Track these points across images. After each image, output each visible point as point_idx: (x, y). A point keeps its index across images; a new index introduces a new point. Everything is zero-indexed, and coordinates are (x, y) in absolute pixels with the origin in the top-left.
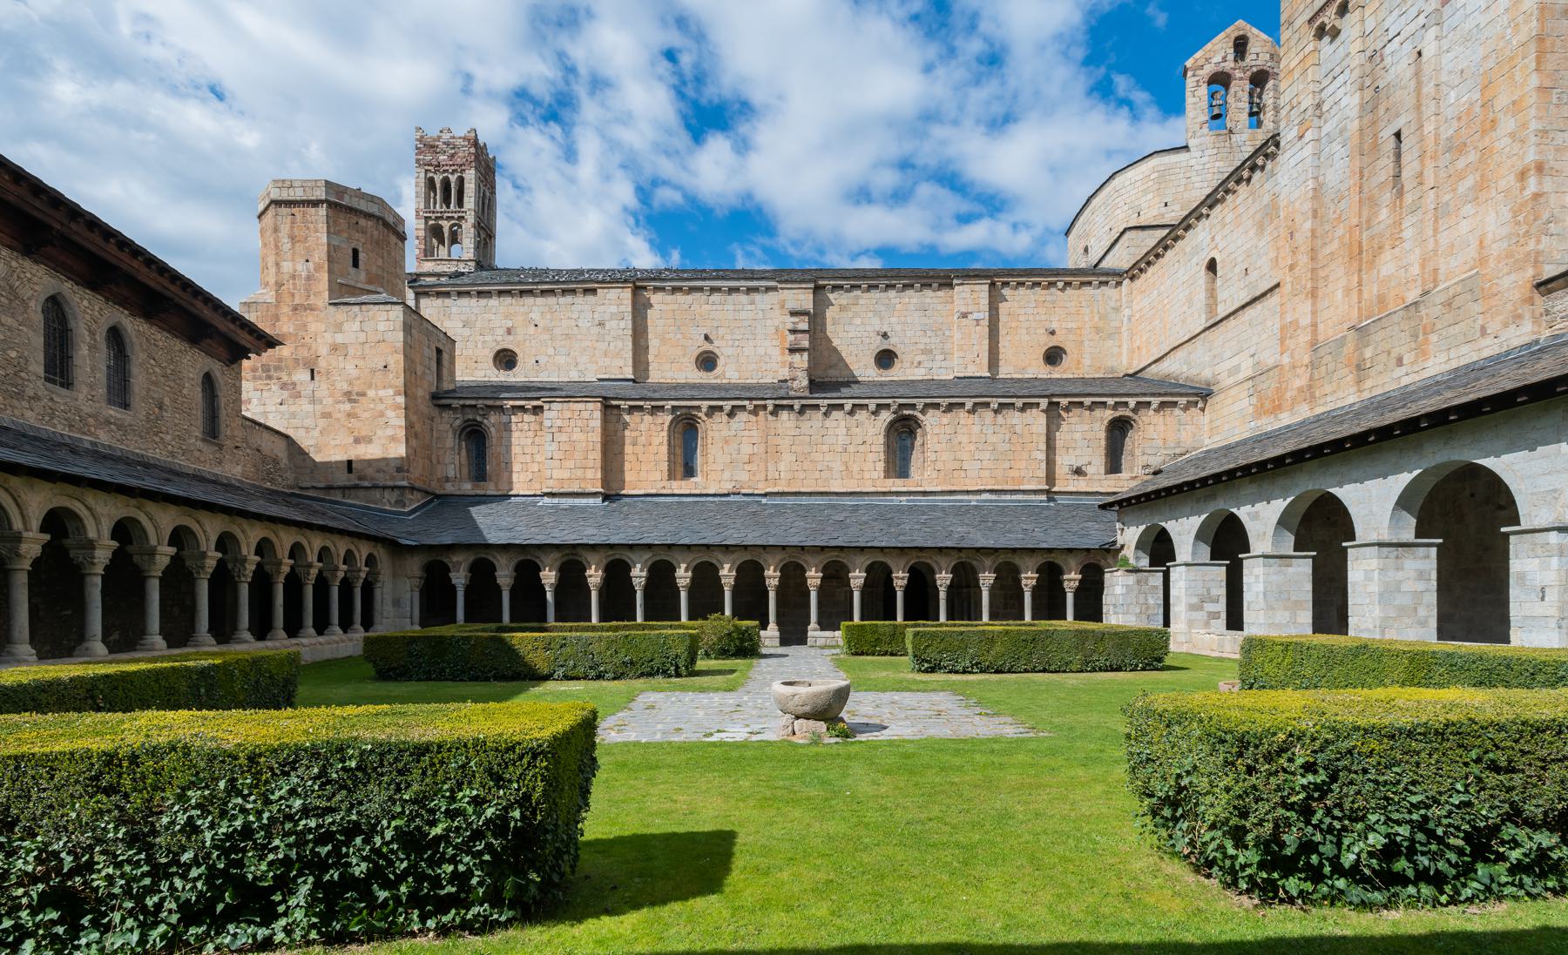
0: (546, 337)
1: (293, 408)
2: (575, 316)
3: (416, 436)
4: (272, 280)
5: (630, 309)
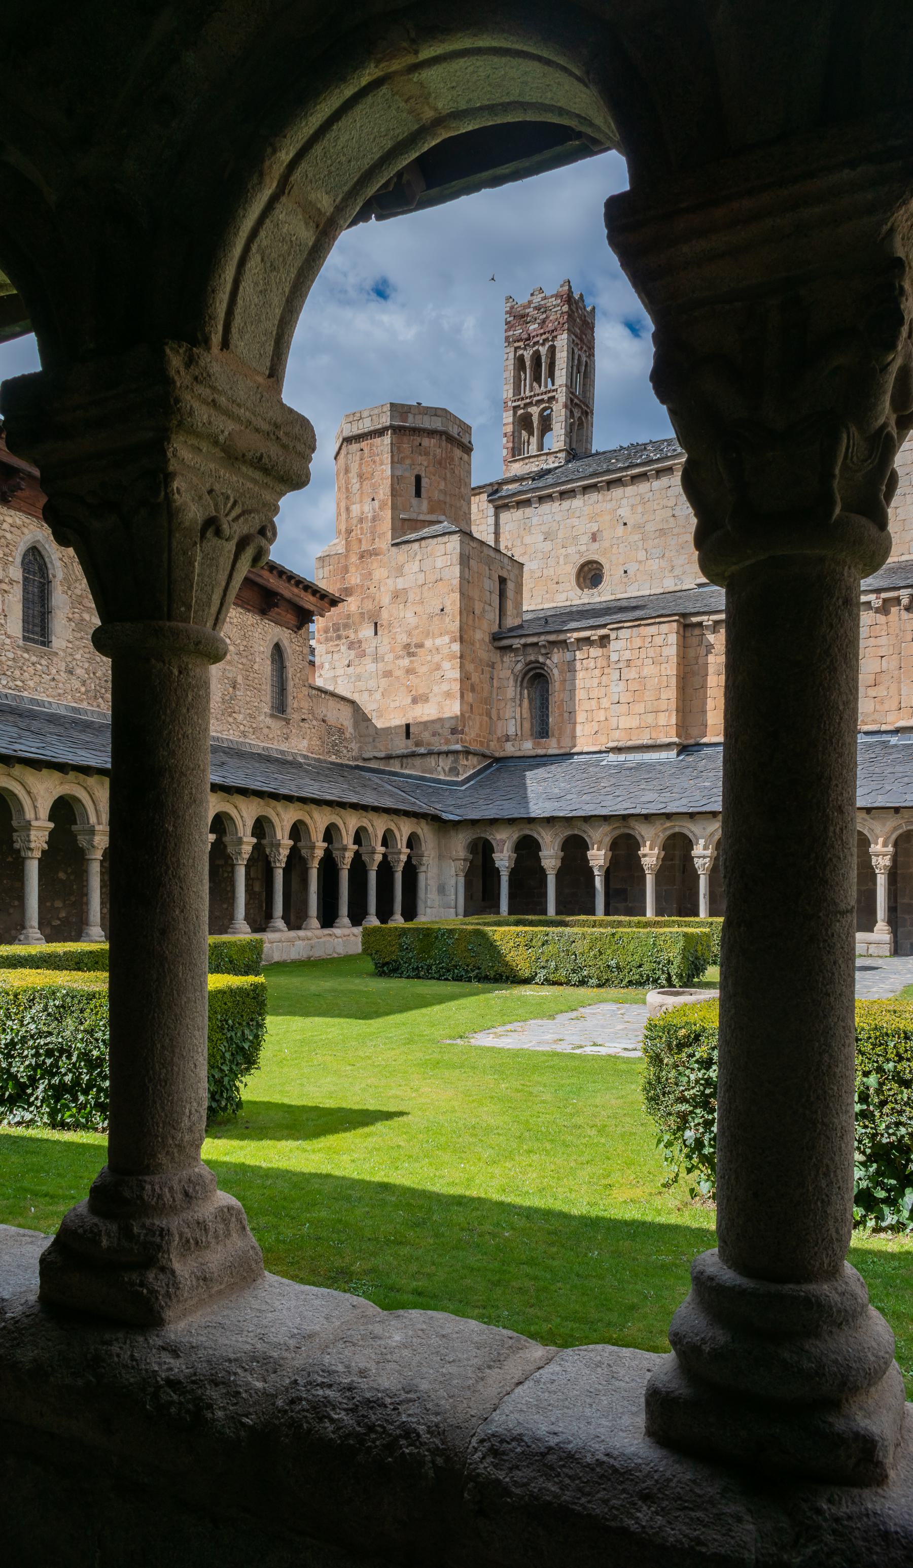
0: (637, 537)
1: (359, 670)
3: (473, 689)
4: (343, 527)
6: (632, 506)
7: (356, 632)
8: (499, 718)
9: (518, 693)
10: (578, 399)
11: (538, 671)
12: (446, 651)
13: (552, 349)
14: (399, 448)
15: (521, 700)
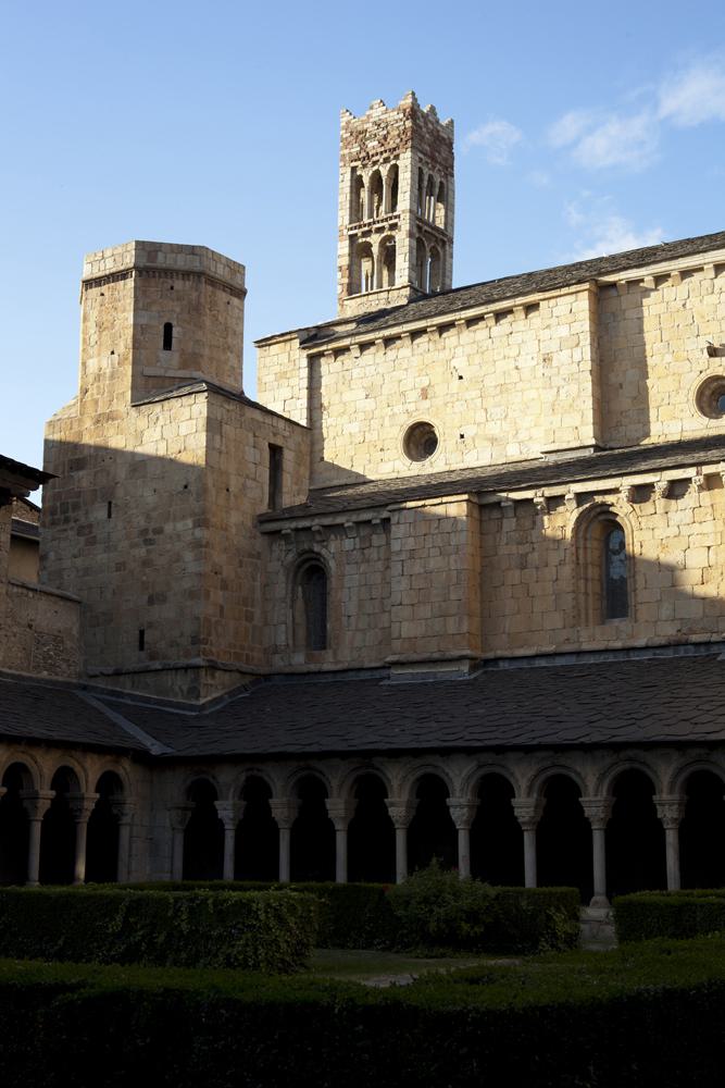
2: (513, 352)
3: (224, 586)
5: (586, 326)
6: (469, 356)
7: (87, 513)
8: (266, 624)
9: (289, 592)
11: (313, 562)
12: (189, 538)
13: (395, 169)
14: (144, 292)
15: (293, 601)
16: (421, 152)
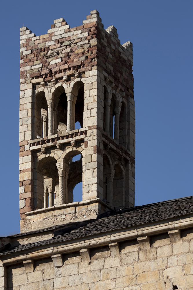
10: (113, 143)
16: (106, 71)
